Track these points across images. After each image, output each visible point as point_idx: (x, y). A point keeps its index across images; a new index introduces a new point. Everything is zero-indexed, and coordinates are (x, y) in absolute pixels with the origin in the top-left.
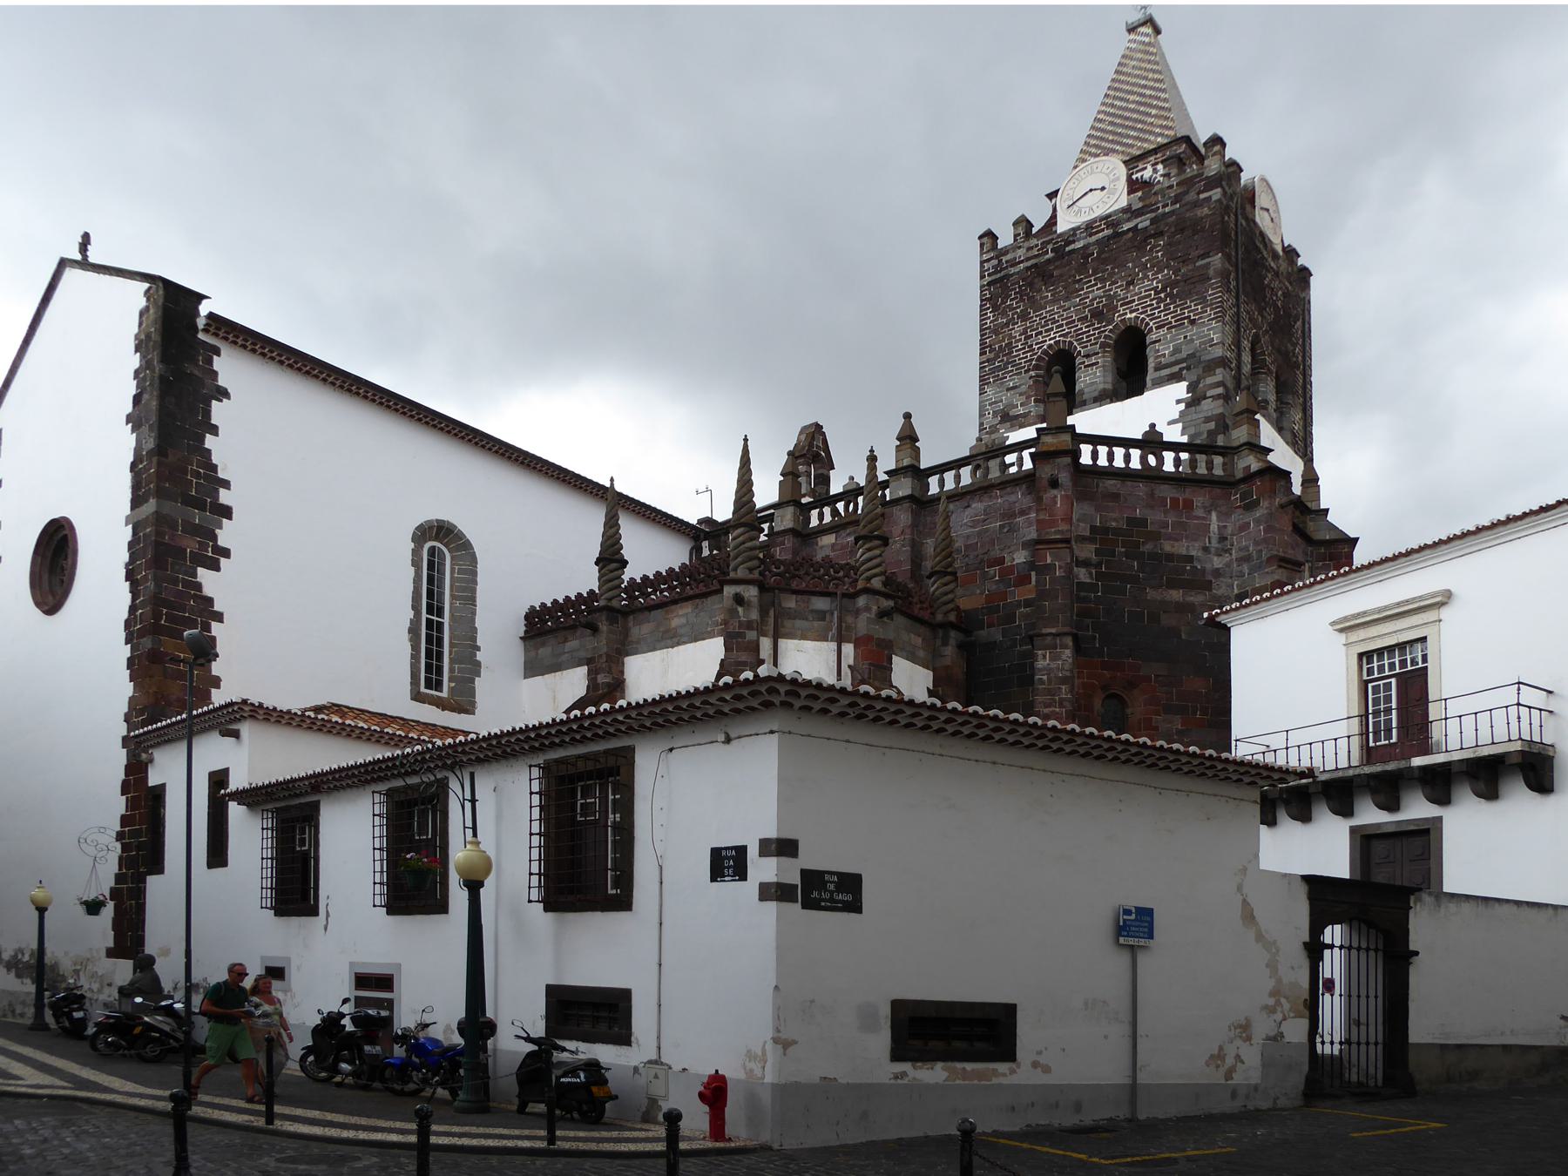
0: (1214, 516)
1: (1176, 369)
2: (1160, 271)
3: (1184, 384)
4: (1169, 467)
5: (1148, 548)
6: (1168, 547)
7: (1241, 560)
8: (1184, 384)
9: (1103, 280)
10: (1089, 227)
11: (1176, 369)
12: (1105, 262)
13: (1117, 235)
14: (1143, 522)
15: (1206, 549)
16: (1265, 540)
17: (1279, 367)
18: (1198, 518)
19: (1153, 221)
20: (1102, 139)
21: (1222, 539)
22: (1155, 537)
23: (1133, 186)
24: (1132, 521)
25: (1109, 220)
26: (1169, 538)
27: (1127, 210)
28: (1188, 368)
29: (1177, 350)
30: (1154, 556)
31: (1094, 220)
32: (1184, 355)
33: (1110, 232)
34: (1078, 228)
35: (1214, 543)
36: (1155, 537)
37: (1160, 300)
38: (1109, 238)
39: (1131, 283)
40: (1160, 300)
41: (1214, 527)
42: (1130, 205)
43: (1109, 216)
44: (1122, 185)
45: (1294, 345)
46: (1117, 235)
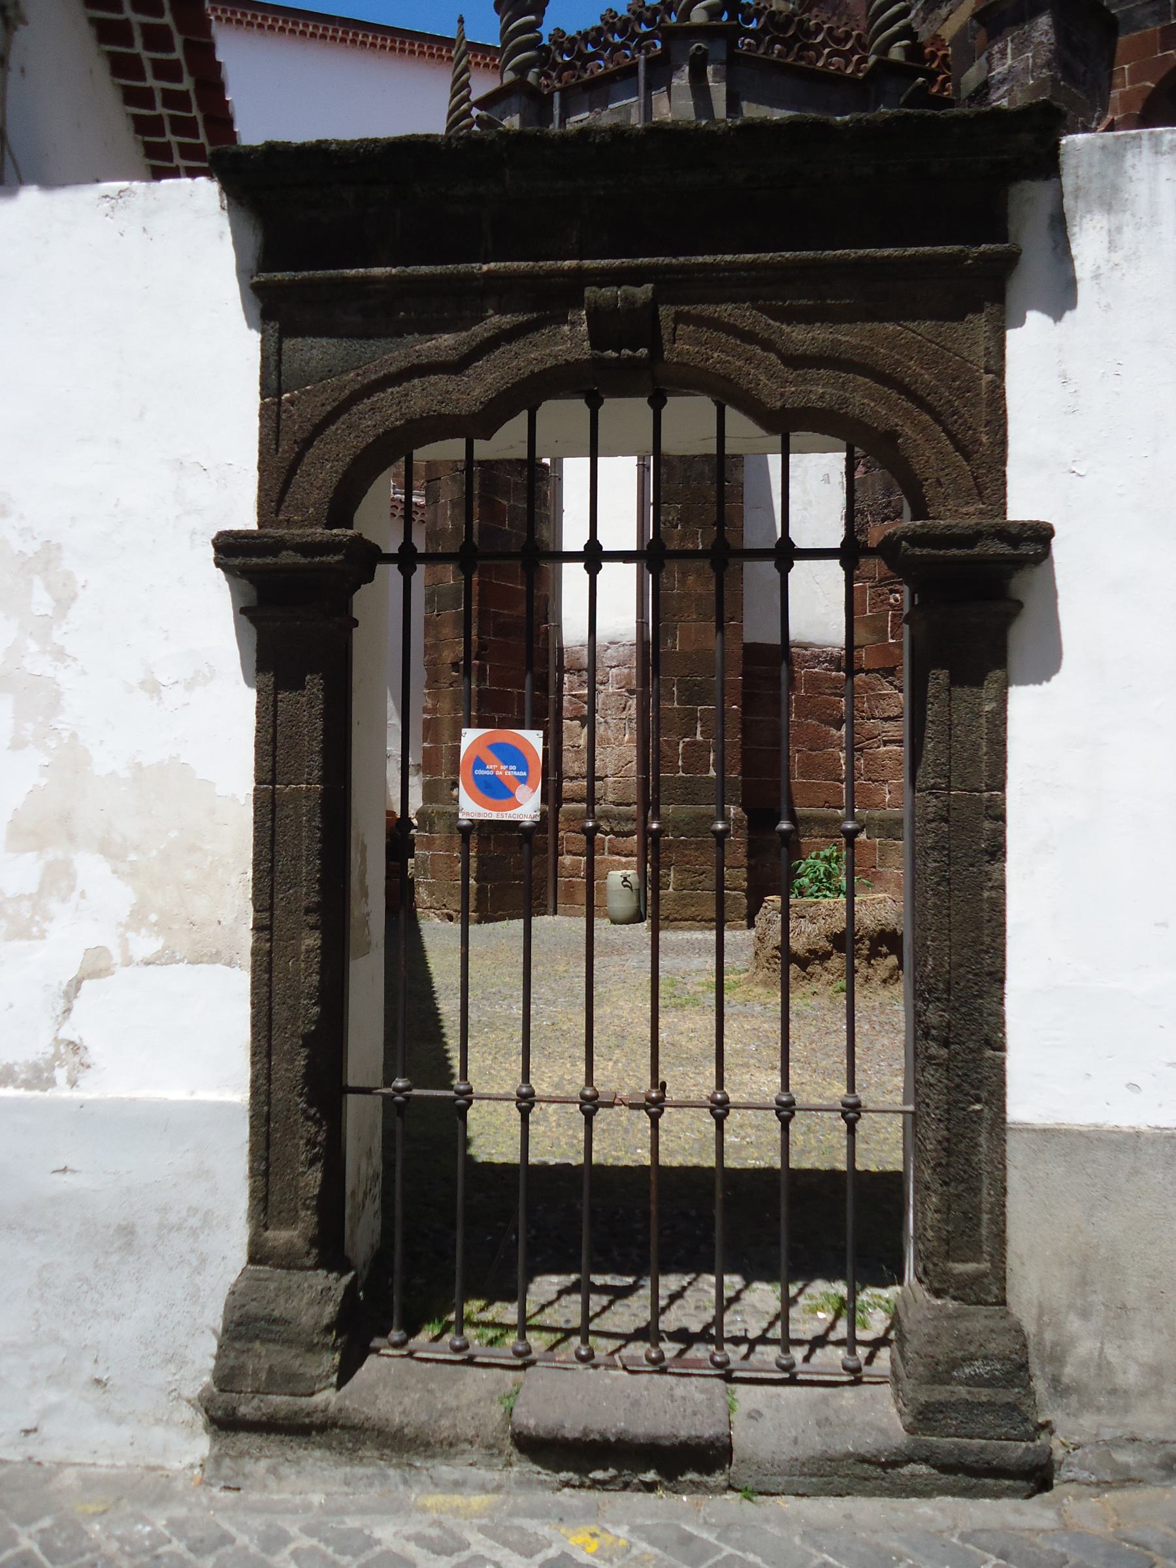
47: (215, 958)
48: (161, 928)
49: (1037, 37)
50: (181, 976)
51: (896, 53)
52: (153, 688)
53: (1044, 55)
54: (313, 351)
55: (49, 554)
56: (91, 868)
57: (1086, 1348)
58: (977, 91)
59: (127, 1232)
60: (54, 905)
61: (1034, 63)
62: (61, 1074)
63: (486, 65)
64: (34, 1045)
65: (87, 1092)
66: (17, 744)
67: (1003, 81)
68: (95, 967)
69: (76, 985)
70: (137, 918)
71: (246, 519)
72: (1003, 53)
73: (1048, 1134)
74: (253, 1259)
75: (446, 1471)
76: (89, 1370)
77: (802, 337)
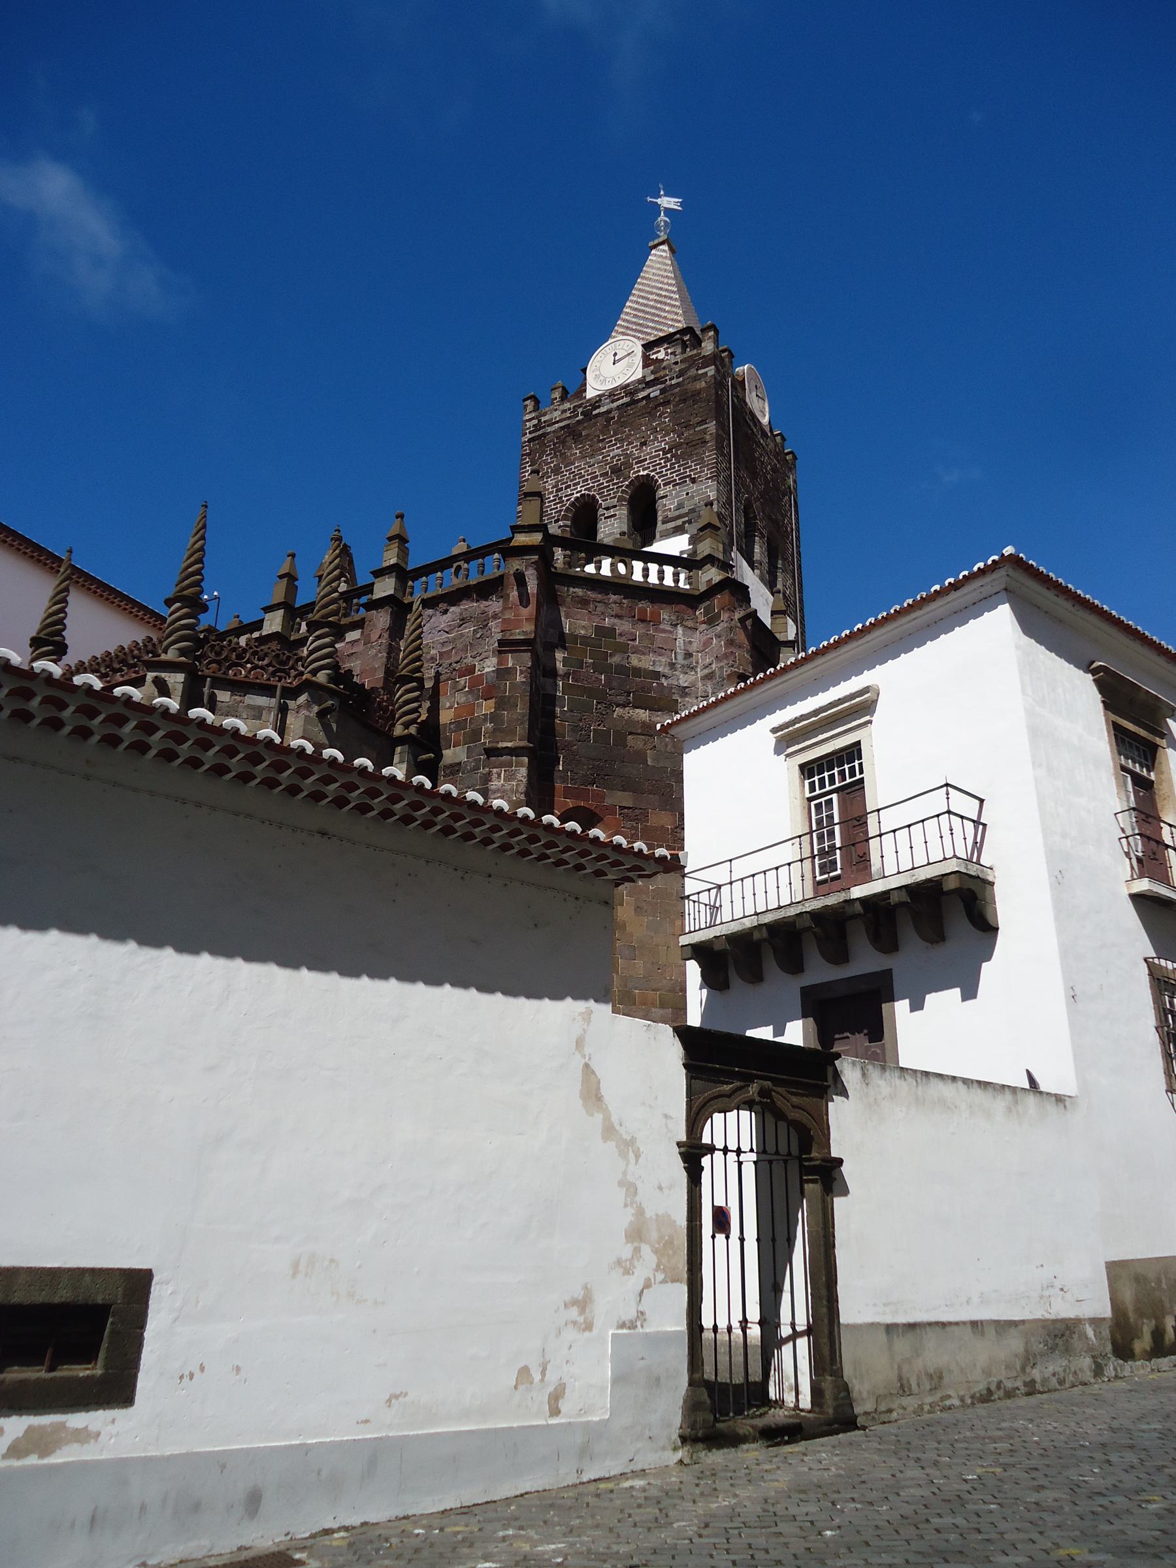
0: (680, 630)
1: (679, 522)
2: (667, 434)
3: (686, 537)
4: (637, 576)
5: (616, 659)
6: (635, 661)
7: (703, 678)
8: (686, 537)
9: (621, 440)
10: (612, 394)
11: (679, 522)
12: (624, 425)
13: (634, 402)
14: (611, 632)
15: (672, 666)
16: (726, 656)
17: (770, 533)
18: (664, 631)
19: (663, 391)
20: (627, 328)
21: (688, 655)
22: (623, 649)
23: (647, 362)
24: (600, 630)
25: (628, 389)
26: (636, 651)
27: (641, 381)
28: (690, 522)
29: (680, 506)
30: (622, 670)
31: (615, 389)
32: (686, 510)
33: (625, 400)
34: (603, 395)
35: (680, 658)
36: (623, 649)
37: (667, 460)
38: (627, 405)
39: (644, 444)
40: (667, 460)
41: (680, 642)
42: (644, 377)
43: (628, 385)
44: (638, 359)
45: (784, 516)
46: (634, 402)
47: (677, 1281)
48: (664, 1271)
49: (519, 776)
50: (670, 1286)
51: (413, 730)
52: (660, 1188)
53: (522, 788)
54: (698, 1084)
55: (633, 1141)
56: (646, 1250)
57: (856, 1388)
58: (452, 766)
59: (658, 1379)
60: (636, 1263)
61: (517, 791)
62: (639, 1324)
63: (52, 568)
64: (630, 1314)
65: (648, 1329)
66: (626, 1205)
67: (498, 790)
68: (647, 1285)
69: (642, 1292)
70: (657, 1269)
71: (683, 1138)
72: (499, 775)
73: (847, 1326)
74: (690, 1385)
75: (745, 1446)
76: (647, 1433)
77: (795, 1100)
